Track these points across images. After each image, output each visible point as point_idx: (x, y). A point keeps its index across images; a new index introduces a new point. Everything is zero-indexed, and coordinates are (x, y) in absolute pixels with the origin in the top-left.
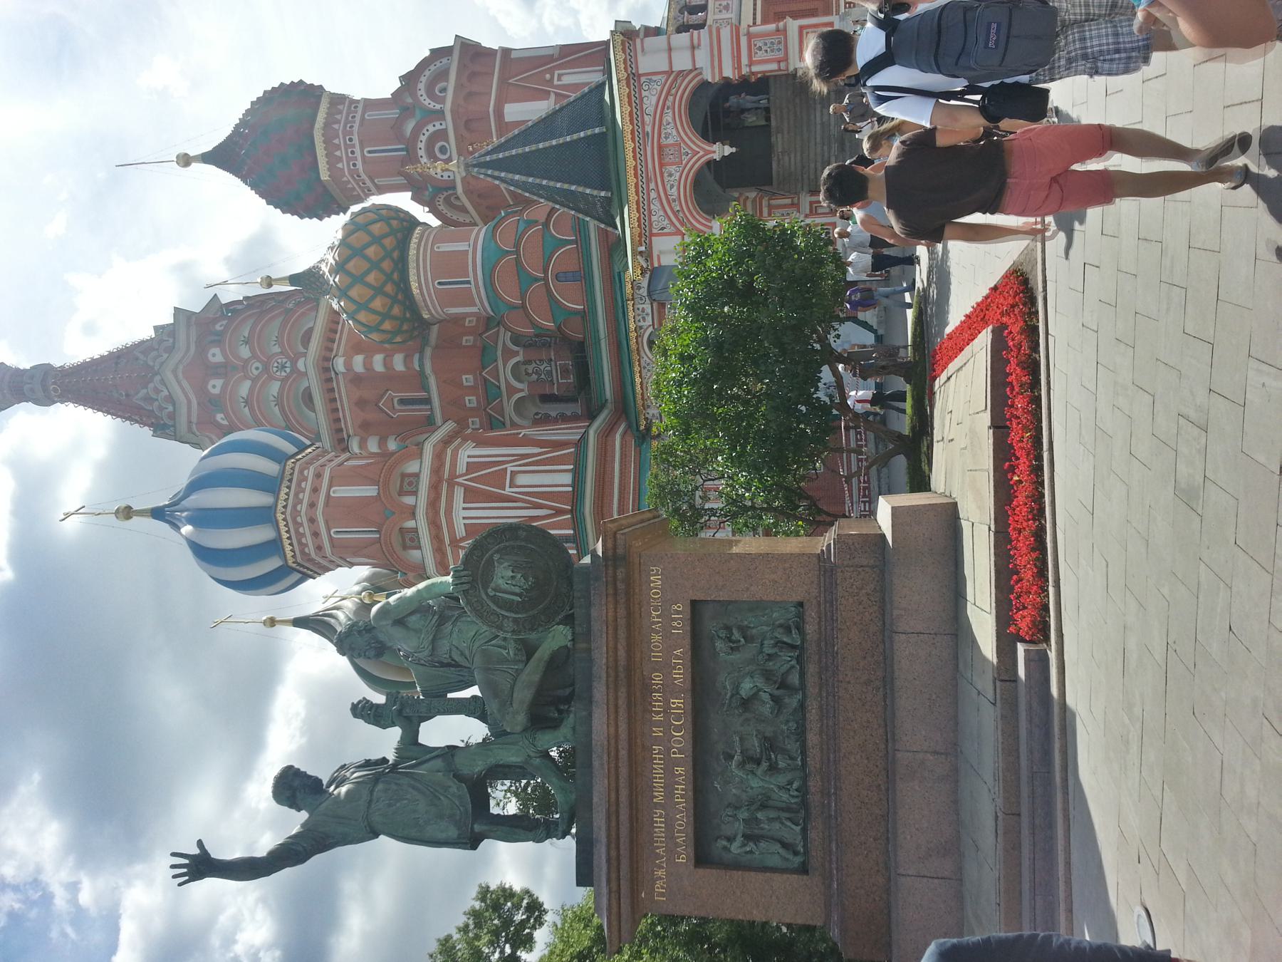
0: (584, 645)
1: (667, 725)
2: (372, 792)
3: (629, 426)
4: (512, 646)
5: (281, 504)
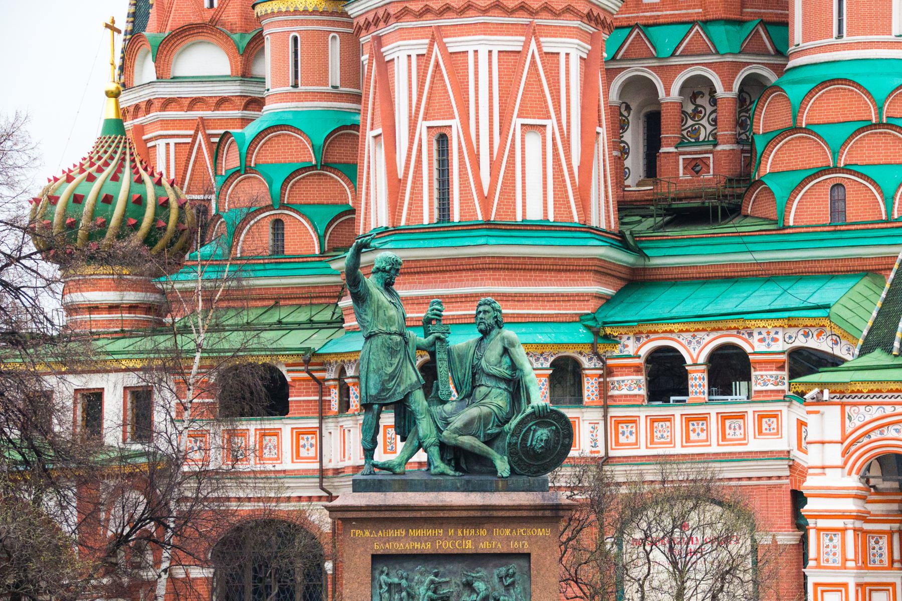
1: (455, 538)
2: (395, 333)
3: (608, 301)
4: (496, 430)
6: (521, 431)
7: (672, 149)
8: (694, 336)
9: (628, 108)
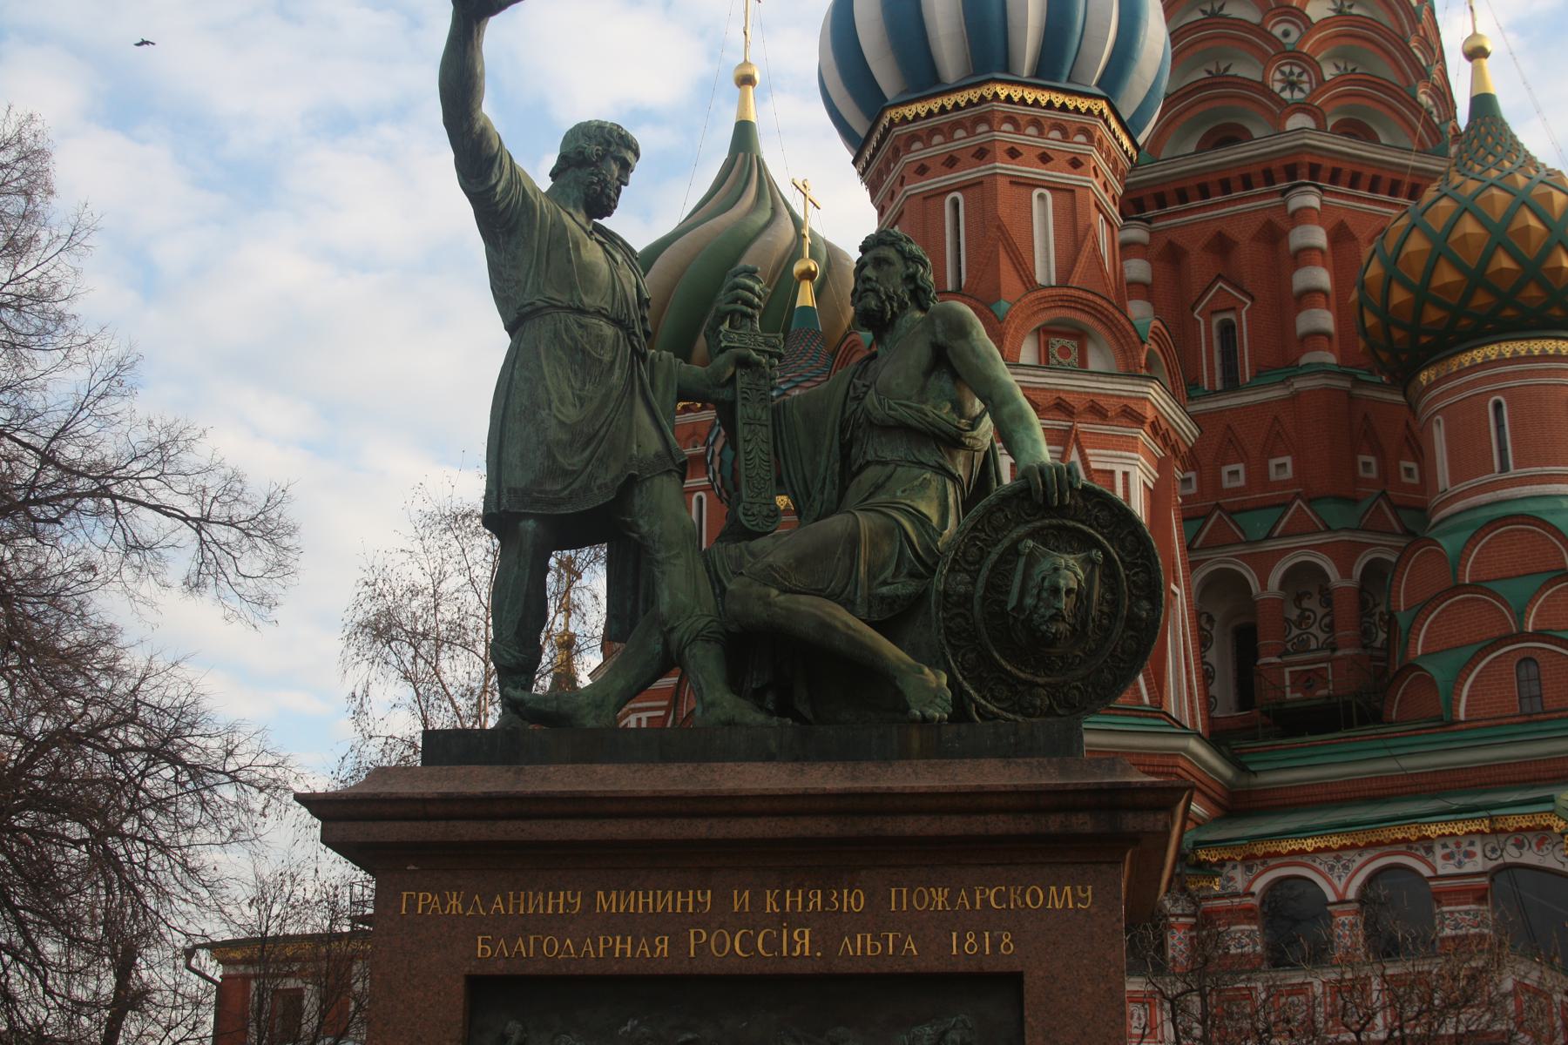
0: (915, 744)
5: (1017, 93)
6: (983, 554)
7: (1274, 660)
8: (1338, 859)
9: (1210, 619)
